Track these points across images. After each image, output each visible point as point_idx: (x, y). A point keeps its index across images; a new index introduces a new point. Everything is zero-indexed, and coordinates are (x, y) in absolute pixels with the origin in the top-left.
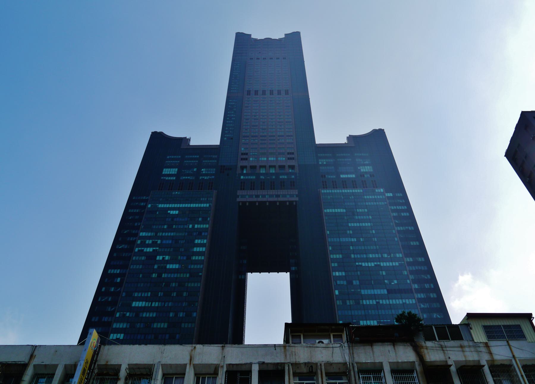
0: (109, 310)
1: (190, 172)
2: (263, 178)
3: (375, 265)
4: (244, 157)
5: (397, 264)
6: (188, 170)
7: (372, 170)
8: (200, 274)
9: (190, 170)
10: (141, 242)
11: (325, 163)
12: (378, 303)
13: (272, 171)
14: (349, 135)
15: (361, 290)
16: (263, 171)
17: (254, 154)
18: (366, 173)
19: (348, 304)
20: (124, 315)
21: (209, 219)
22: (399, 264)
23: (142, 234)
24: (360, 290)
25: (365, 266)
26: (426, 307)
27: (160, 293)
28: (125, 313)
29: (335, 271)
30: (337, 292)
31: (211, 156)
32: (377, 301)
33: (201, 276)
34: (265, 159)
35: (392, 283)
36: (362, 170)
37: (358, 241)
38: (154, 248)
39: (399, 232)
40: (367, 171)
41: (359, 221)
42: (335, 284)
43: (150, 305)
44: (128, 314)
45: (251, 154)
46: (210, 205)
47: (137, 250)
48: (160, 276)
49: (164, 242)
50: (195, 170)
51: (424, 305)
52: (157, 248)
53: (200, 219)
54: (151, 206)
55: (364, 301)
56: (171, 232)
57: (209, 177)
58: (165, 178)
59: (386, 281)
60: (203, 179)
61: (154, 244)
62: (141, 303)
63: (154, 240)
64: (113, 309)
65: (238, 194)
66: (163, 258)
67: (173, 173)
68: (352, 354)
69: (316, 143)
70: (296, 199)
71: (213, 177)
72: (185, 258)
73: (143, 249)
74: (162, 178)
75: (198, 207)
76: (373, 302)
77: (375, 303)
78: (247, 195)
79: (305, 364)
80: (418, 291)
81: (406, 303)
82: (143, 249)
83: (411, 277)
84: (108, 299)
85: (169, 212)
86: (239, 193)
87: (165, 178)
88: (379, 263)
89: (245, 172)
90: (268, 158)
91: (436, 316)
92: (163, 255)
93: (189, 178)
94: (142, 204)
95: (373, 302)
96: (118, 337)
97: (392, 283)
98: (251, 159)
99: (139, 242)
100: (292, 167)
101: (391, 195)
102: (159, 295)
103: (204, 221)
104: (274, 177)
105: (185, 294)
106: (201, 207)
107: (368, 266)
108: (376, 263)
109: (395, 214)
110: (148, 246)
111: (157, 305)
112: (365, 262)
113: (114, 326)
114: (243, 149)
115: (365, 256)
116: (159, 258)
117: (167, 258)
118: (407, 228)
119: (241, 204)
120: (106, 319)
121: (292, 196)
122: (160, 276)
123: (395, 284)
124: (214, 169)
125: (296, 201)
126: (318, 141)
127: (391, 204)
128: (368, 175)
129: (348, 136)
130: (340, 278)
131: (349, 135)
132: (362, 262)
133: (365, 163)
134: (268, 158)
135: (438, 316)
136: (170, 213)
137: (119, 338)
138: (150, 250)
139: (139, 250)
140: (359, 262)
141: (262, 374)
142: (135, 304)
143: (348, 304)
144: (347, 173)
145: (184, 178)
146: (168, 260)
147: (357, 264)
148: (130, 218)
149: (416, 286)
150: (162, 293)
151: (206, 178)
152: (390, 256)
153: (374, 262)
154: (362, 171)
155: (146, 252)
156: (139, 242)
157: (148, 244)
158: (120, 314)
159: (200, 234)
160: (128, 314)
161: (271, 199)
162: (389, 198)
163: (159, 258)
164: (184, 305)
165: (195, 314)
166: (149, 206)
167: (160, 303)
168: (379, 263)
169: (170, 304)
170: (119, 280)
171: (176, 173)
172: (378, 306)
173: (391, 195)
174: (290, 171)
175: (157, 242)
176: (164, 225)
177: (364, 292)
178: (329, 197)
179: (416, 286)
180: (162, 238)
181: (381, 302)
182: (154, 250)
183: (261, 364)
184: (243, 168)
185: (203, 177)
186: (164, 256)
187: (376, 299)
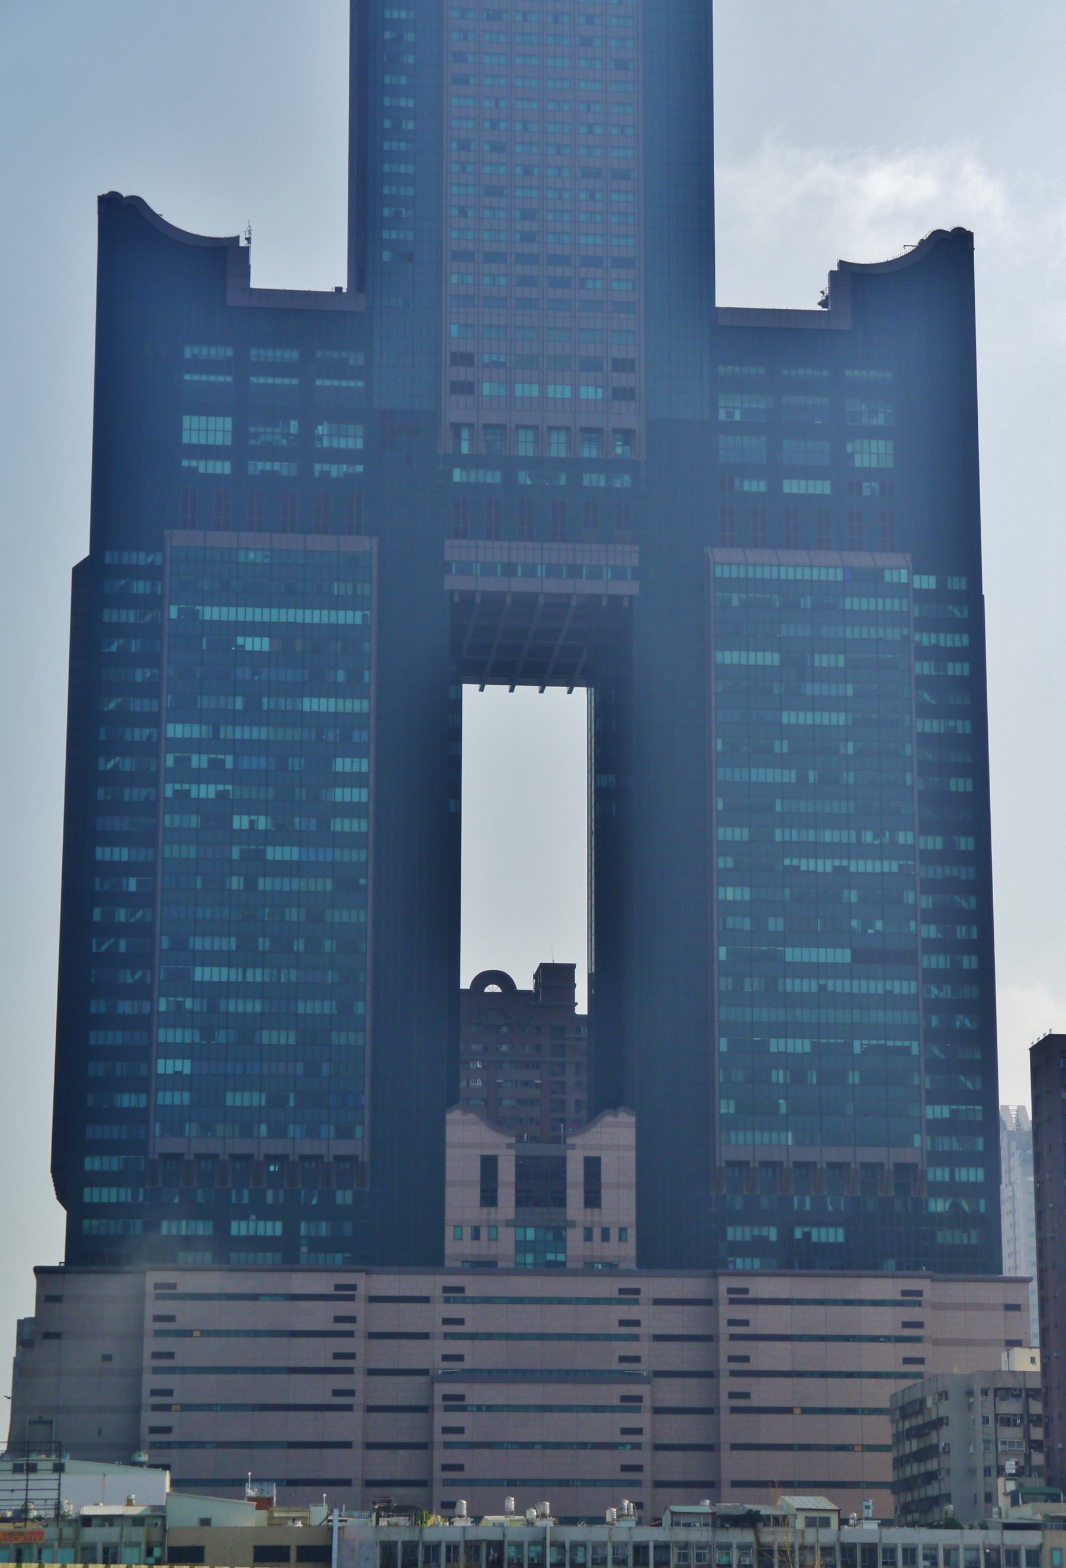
0: (130, 981)
1: (278, 437)
2: (529, 482)
3: (834, 867)
4: (462, 373)
5: (895, 868)
6: (269, 430)
7: (890, 463)
8: (362, 881)
9: (277, 430)
10: (176, 759)
11: (737, 417)
12: (822, 988)
13: (558, 448)
14: (842, 263)
15: (785, 947)
16: (525, 447)
17: (494, 358)
18: (870, 473)
19: (746, 990)
20: (179, 1005)
21: (366, 674)
22: (901, 867)
23: (175, 730)
24: (782, 949)
25: (808, 872)
26: (942, 995)
27: (261, 940)
28: (179, 999)
29: (726, 884)
30: (722, 953)
31: (344, 354)
32: (822, 982)
33: (365, 887)
34: (535, 390)
35: (870, 931)
36: (858, 463)
37: (802, 779)
38: (220, 787)
39: (924, 740)
40: (874, 465)
41: (815, 704)
42: (721, 928)
43: (240, 979)
44: (188, 1004)
45: (486, 359)
46: (364, 617)
47: (169, 790)
48: (251, 884)
49: (245, 763)
50: (294, 427)
51: (940, 989)
52: (229, 787)
53: (341, 676)
54: (180, 611)
55: (789, 982)
56: (260, 725)
57: (345, 468)
58: (194, 463)
59: (854, 923)
60: (326, 474)
61: (215, 772)
62: (216, 970)
63: (213, 756)
64: (138, 975)
65: (448, 557)
66: (252, 823)
67: (219, 442)
68: (714, 1536)
69: (717, 305)
70: (628, 588)
71: (360, 468)
72: (313, 825)
73: (186, 787)
74: (185, 463)
75: (329, 626)
76: (809, 986)
77: (814, 989)
78: (477, 562)
79: (683, 1542)
80: (931, 947)
81: (891, 991)
82: (186, 787)
83: (926, 902)
84: (116, 945)
85: (240, 640)
86: (455, 550)
87: (194, 463)
88: (845, 863)
89: (465, 448)
90: (543, 385)
91: (963, 1023)
92: (248, 814)
93: (277, 466)
94: (140, 587)
95: (809, 986)
96: (178, 1068)
97: (870, 931)
98: (486, 389)
99: (170, 761)
100: (627, 435)
101: (928, 582)
102: (261, 949)
103: (352, 688)
104: (563, 480)
105: (328, 945)
106: (337, 626)
107: (815, 872)
108: (837, 863)
109: (926, 668)
110: (199, 777)
111: (259, 979)
112: (807, 856)
113: (166, 1035)
114: (454, 330)
115: (811, 836)
116: (241, 822)
117: (262, 823)
118: (951, 723)
119: (456, 599)
120: (125, 1007)
121: (619, 574)
122: (251, 884)
123: (877, 932)
124: (360, 429)
125: (631, 597)
126: (724, 298)
127: (922, 625)
128: (874, 484)
129: (836, 268)
130: (735, 907)
131: (842, 263)
132: (800, 857)
133: (874, 422)
134: (543, 385)
135: (968, 1023)
136: (243, 646)
137: (182, 1072)
138: (207, 791)
139: (176, 793)
140: (792, 857)
141: (656, 1547)
142: (202, 974)
143: (748, 989)
144: (807, 473)
145: (260, 465)
146: (266, 832)
147: (787, 862)
148: (114, 648)
149: (931, 931)
150: (267, 941)
151: (336, 471)
152: (881, 840)
153: (832, 857)
154: (858, 464)
155: (199, 800)
156: (170, 761)
157: (199, 770)
158: (168, 1002)
159: (343, 722)
160: (188, 1004)
161: (552, 586)
162: (921, 596)
163: (241, 822)
164: (330, 981)
165: (360, 1008)
166: (173, 612)
167: (267, 971)
168: (845, 863)
169: (293, 976)
170: (132, 885)
171: (228, 442)
172: (822, 999)
173: (928, 582)
174: (619, 450)
175: (223, 761)
176: (235, 695)
177: (792, 955)
178: (735, 600)
179: (931, 931)
180: (236, 747)
181: (830, 987)
182: (222, 796)
183: (656, 1541)
184: (457, 428)
185: (326, 467)
186: (253, 818)
187: (818, 978)
